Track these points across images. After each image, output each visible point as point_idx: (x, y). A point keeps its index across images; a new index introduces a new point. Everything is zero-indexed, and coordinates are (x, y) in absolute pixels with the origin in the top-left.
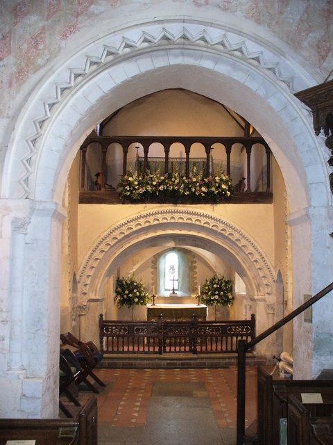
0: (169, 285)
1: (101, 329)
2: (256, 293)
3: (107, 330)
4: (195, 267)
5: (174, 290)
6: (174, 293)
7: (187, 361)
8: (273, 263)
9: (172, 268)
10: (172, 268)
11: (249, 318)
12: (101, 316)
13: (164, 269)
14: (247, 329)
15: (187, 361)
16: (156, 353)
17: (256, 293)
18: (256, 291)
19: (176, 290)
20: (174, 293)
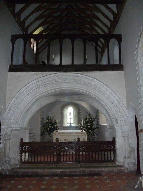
0: (69, 121)
1: (22, 148)
2: (115, 124)
3: (25, 148)
4: (80, 113)
5: (71, 123)
6: (71, 124)
7: (73, 170)
8: (126, 105)
9: (70, 113)
10: (70, 113)
11: (111, 140)
12: (22, 139)
13: (67, 114)
14: (111, 146)
15: (73, 170)
16: (54, 162)
17: (115, 124)
18: (115, 123)
19: (73, 123)
20: (71, 124)
